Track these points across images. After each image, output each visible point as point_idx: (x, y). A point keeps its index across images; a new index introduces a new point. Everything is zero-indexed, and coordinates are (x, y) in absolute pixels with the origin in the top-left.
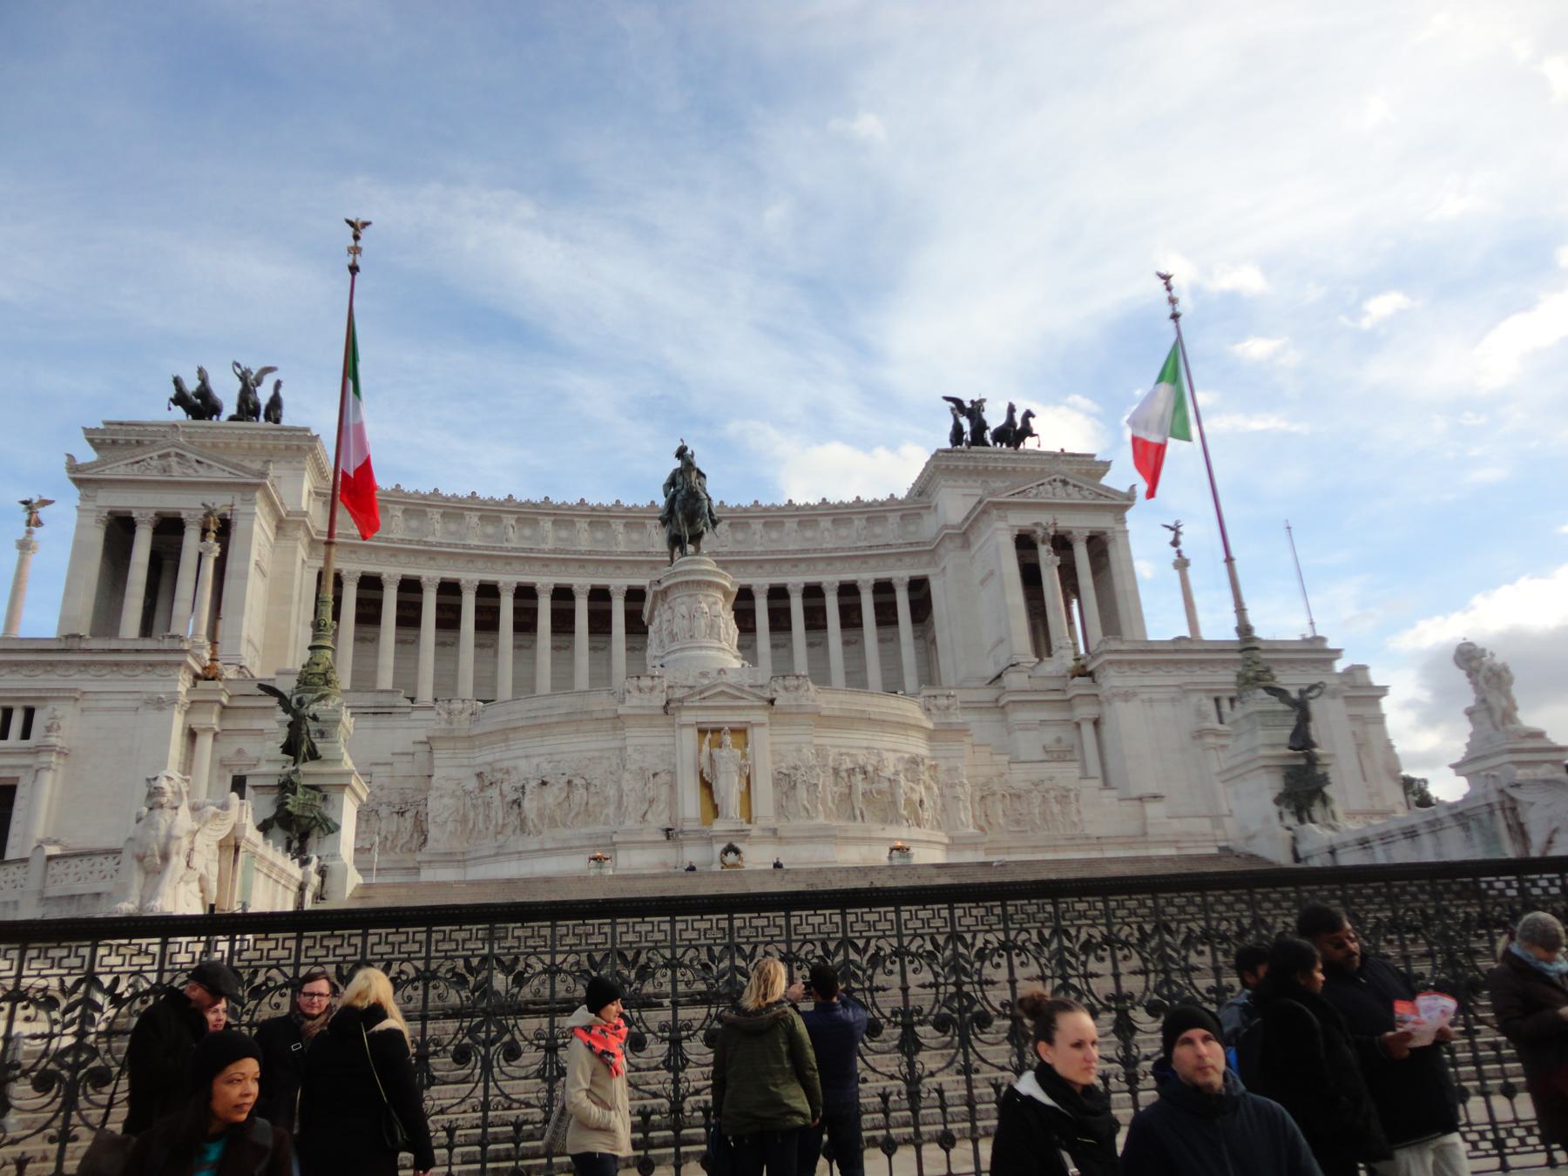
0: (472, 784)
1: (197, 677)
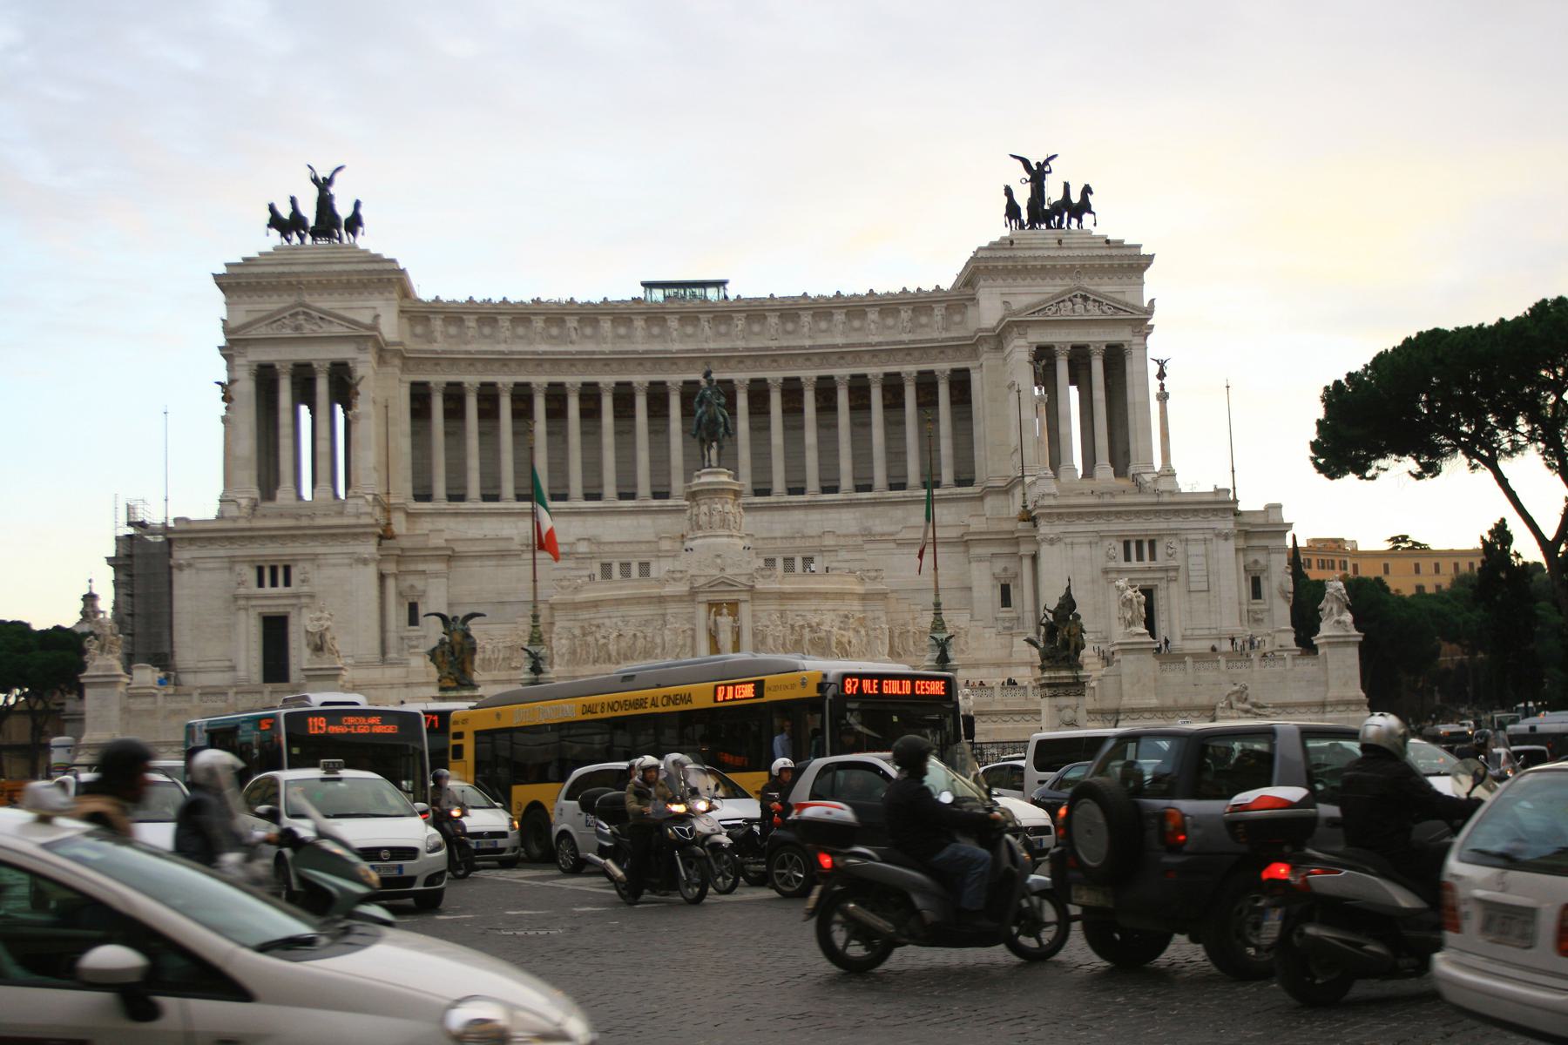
0: (577, 632)
1: (381, 537)
